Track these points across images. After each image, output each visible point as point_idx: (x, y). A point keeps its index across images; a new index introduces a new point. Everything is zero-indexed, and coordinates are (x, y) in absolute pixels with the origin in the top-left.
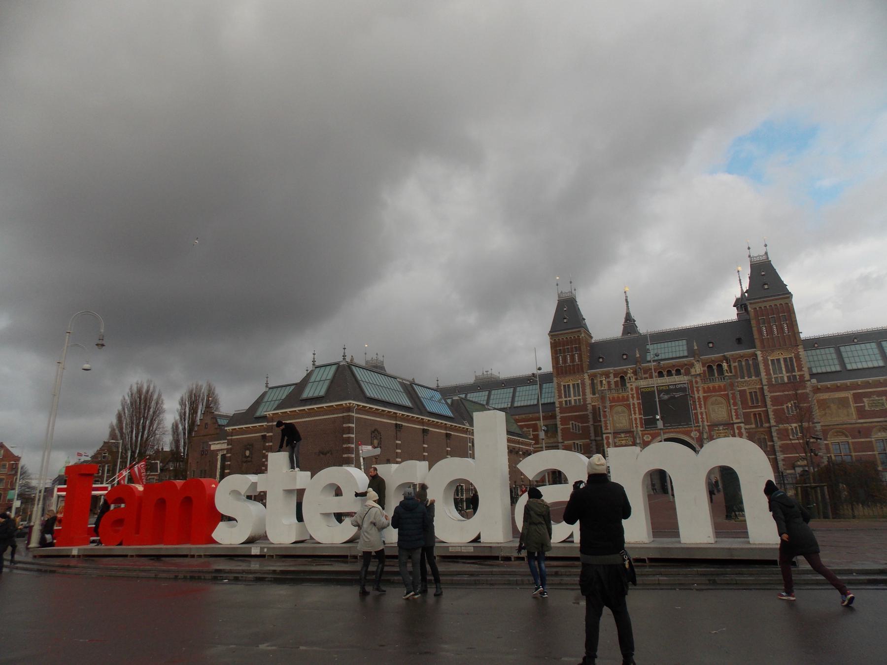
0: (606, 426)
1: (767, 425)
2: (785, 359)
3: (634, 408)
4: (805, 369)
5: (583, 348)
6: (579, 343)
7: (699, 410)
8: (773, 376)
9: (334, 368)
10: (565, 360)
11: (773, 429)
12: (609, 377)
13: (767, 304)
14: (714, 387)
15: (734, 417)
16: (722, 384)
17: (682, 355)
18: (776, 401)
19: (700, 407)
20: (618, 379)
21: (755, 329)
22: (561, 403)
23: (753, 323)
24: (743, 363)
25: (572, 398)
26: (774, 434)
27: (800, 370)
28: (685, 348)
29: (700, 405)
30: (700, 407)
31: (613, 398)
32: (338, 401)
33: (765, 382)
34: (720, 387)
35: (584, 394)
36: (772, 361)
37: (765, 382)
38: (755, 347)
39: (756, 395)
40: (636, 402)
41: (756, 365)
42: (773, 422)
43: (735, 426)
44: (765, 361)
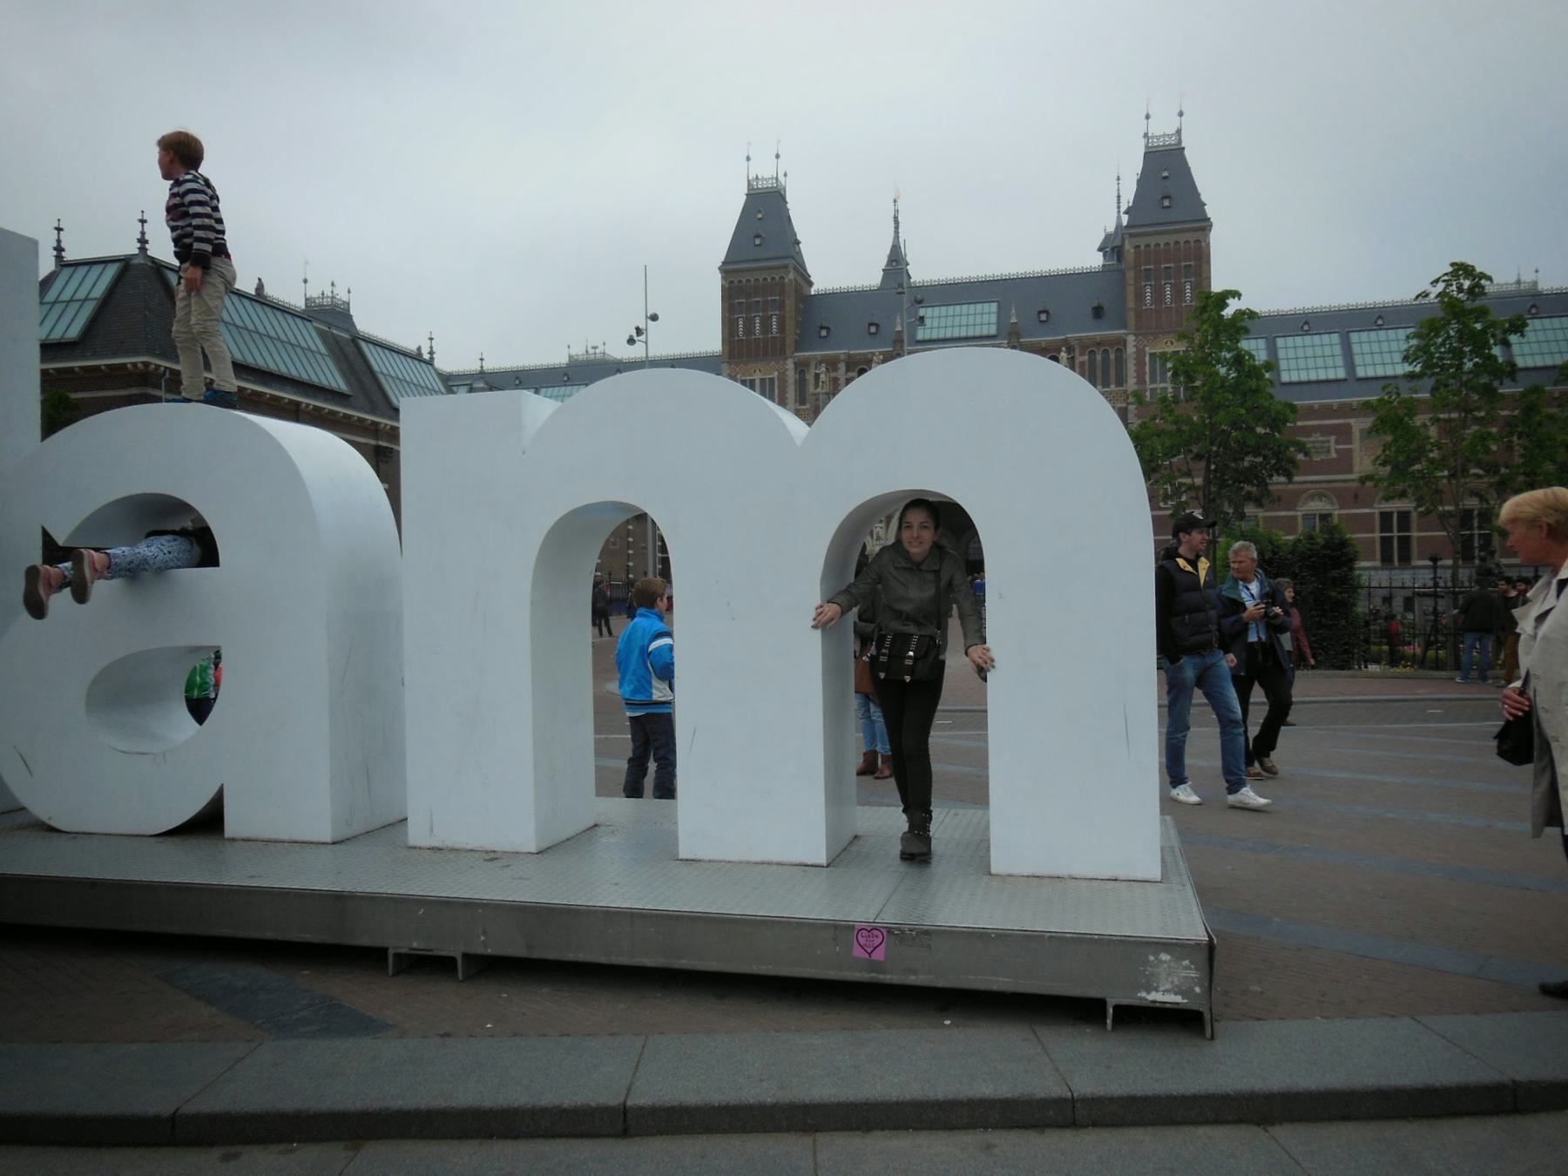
5: (790, 303)
9: (111, 271)
10: (749, 329)
12: (836, 369)
13: (1162, 240)
17: (985, 333)
24: (1099, 358)
28: (994, 318)
32: (115, 355)
41: (1121, 363)
44: (1140, 353)
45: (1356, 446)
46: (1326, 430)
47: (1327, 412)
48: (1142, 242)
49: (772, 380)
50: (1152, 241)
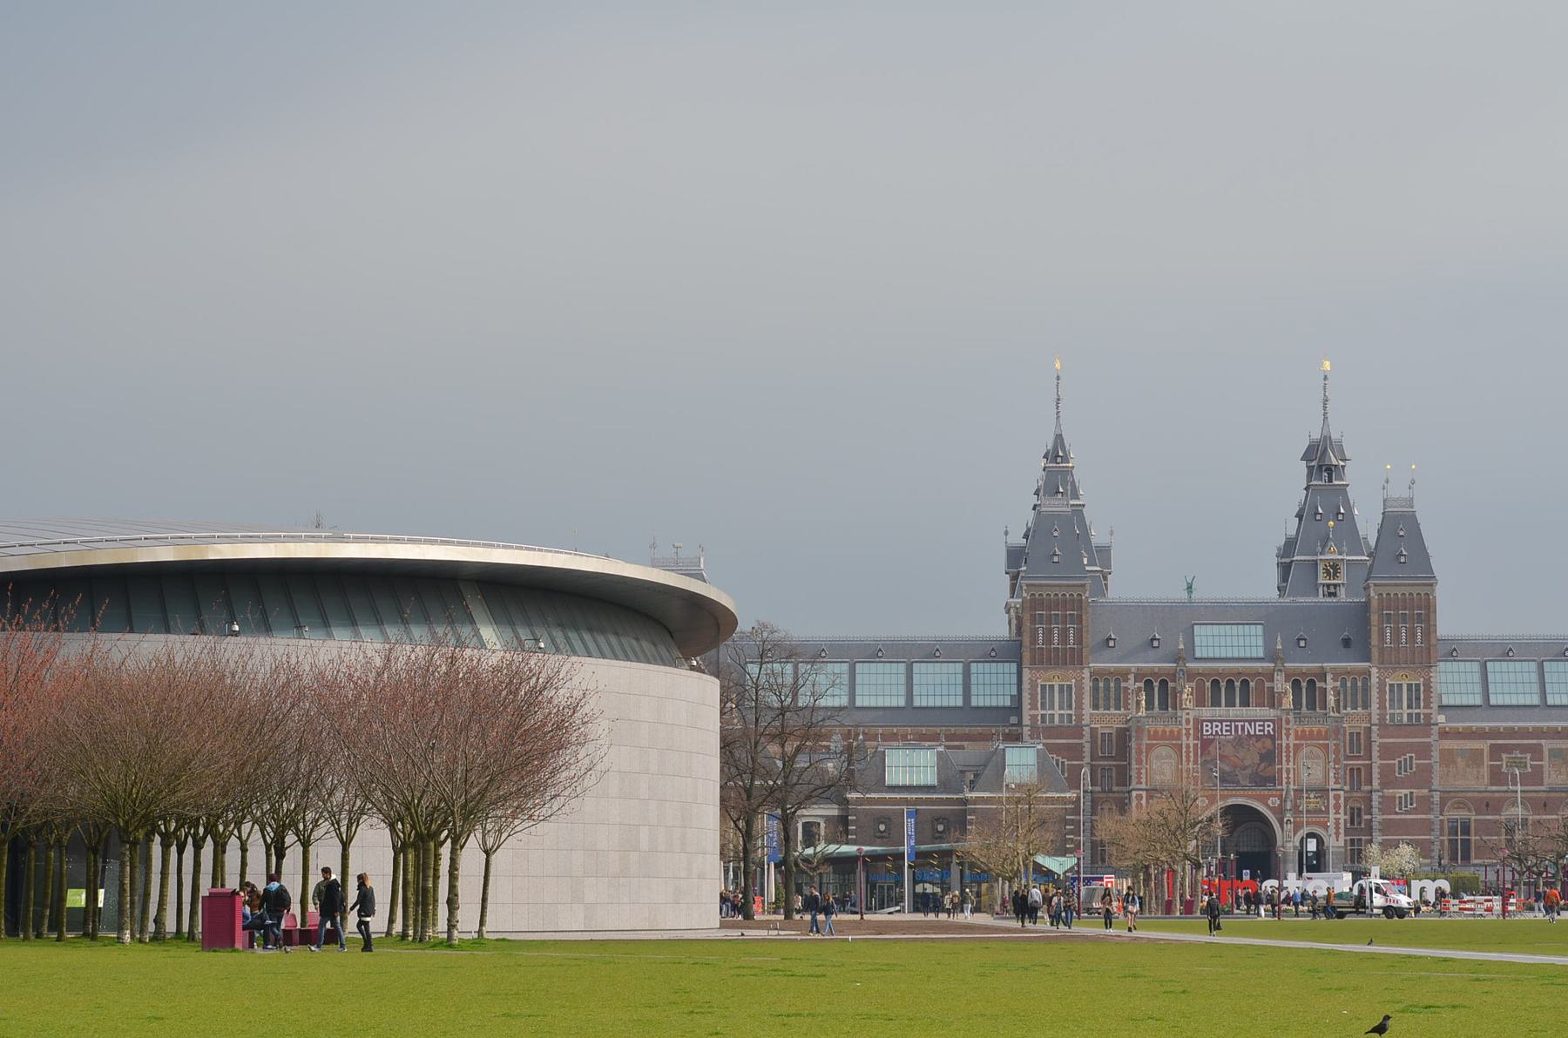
0: (1139, 778)
1: (1366, 788)
2: (1410, 686)
3: (1188, 752)
4: (1435, 706)
6: (1081, 608)
7: (1285, 766)
8: (1389, 711)
11: (1375, 796)
12: (1127, 680)
14: (1311, 732)
15: (1332, 781)
16: (1323, 728)
18: (1386, 751)
19: (1288, 761)
20: (1142, 685)
21: (1374, 630)
22: (1033, 718)
23: (1374, 618)
25: (1057, 712)
26: (1375, 803)
27: (1427, 706)
28: (1260, 642)
29: (1288, 757)
30: (1288, 761)
31: (1156, 732)
33: (1375, 719)
34: (1319, 732)
35: (1080, 706)
36: (1392, 686)
37: (1375, 719)
38: (1369, 659)
39: (1358, 740)
40: (1191, 742)
41: (1366, 689)
42: (1376, 784)
43: (1331, 794)
44: (1382, 684)
45: (1545, 763)
46: (1524, 749)
47: (1524, 733)
48: (1384, 591)
49: (1070, 687)
50: (1392, 591)
